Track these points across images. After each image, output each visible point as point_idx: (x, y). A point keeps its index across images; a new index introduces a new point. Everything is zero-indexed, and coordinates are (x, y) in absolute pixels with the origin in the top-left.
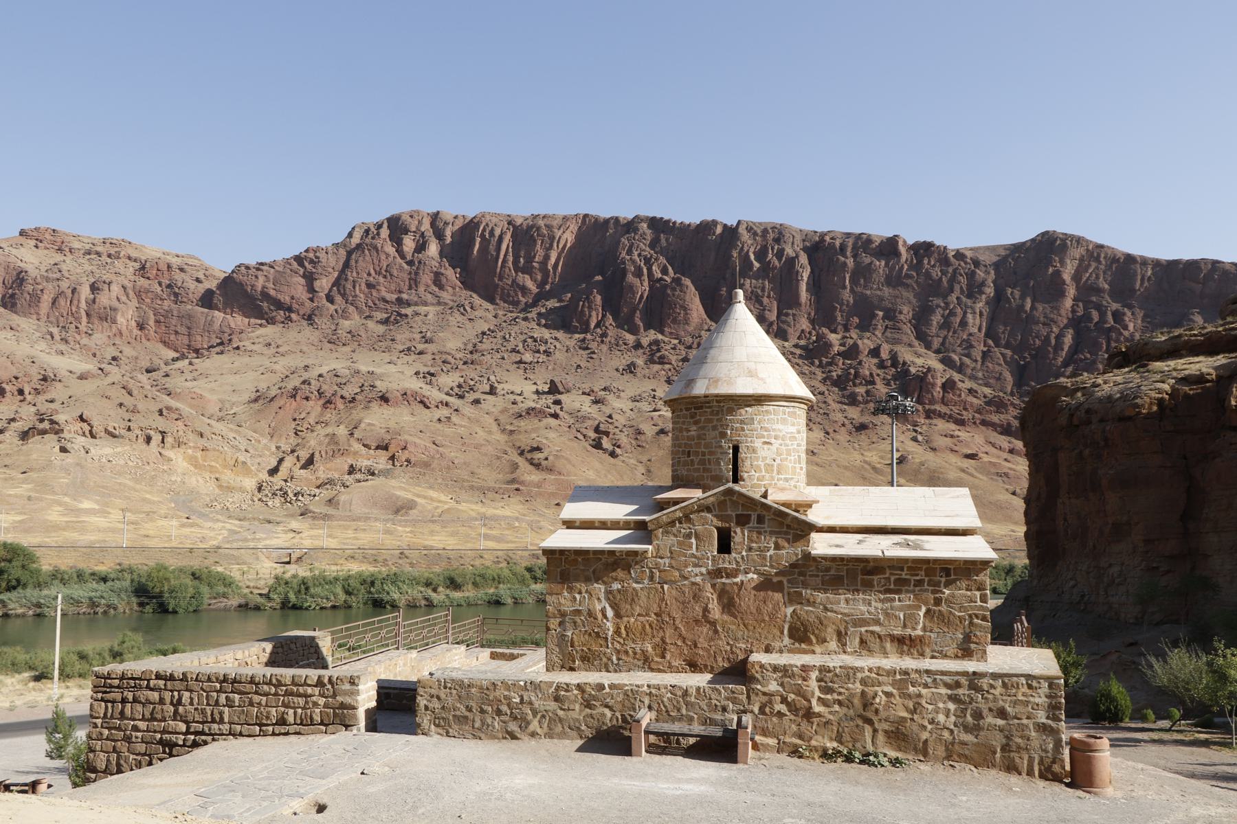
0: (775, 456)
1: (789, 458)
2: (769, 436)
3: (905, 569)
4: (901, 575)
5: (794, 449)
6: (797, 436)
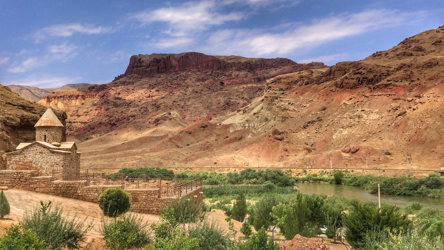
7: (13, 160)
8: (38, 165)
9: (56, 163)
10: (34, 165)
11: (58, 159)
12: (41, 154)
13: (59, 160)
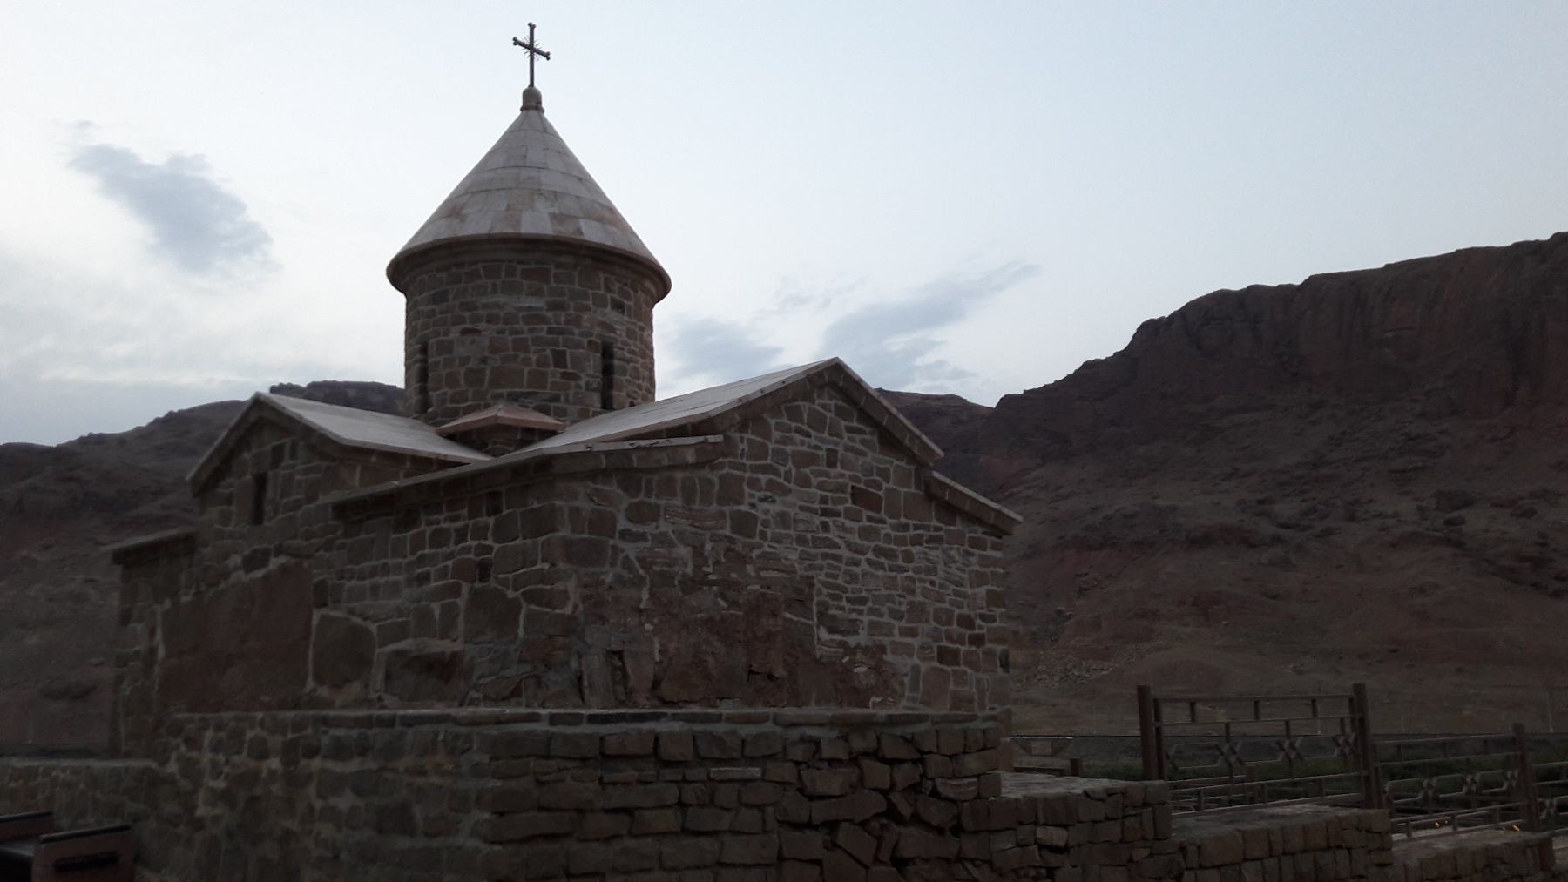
0: (486, 354)
1: (522, 355)
2: (476, 319)
5: (537, 341)
6: (550, 315)
7: (631, 550)
8: (852, 641)
9: (966, 622)
10: (824, 634)
11: (980, 579)
12: (866, 513)
13: (982, 591)
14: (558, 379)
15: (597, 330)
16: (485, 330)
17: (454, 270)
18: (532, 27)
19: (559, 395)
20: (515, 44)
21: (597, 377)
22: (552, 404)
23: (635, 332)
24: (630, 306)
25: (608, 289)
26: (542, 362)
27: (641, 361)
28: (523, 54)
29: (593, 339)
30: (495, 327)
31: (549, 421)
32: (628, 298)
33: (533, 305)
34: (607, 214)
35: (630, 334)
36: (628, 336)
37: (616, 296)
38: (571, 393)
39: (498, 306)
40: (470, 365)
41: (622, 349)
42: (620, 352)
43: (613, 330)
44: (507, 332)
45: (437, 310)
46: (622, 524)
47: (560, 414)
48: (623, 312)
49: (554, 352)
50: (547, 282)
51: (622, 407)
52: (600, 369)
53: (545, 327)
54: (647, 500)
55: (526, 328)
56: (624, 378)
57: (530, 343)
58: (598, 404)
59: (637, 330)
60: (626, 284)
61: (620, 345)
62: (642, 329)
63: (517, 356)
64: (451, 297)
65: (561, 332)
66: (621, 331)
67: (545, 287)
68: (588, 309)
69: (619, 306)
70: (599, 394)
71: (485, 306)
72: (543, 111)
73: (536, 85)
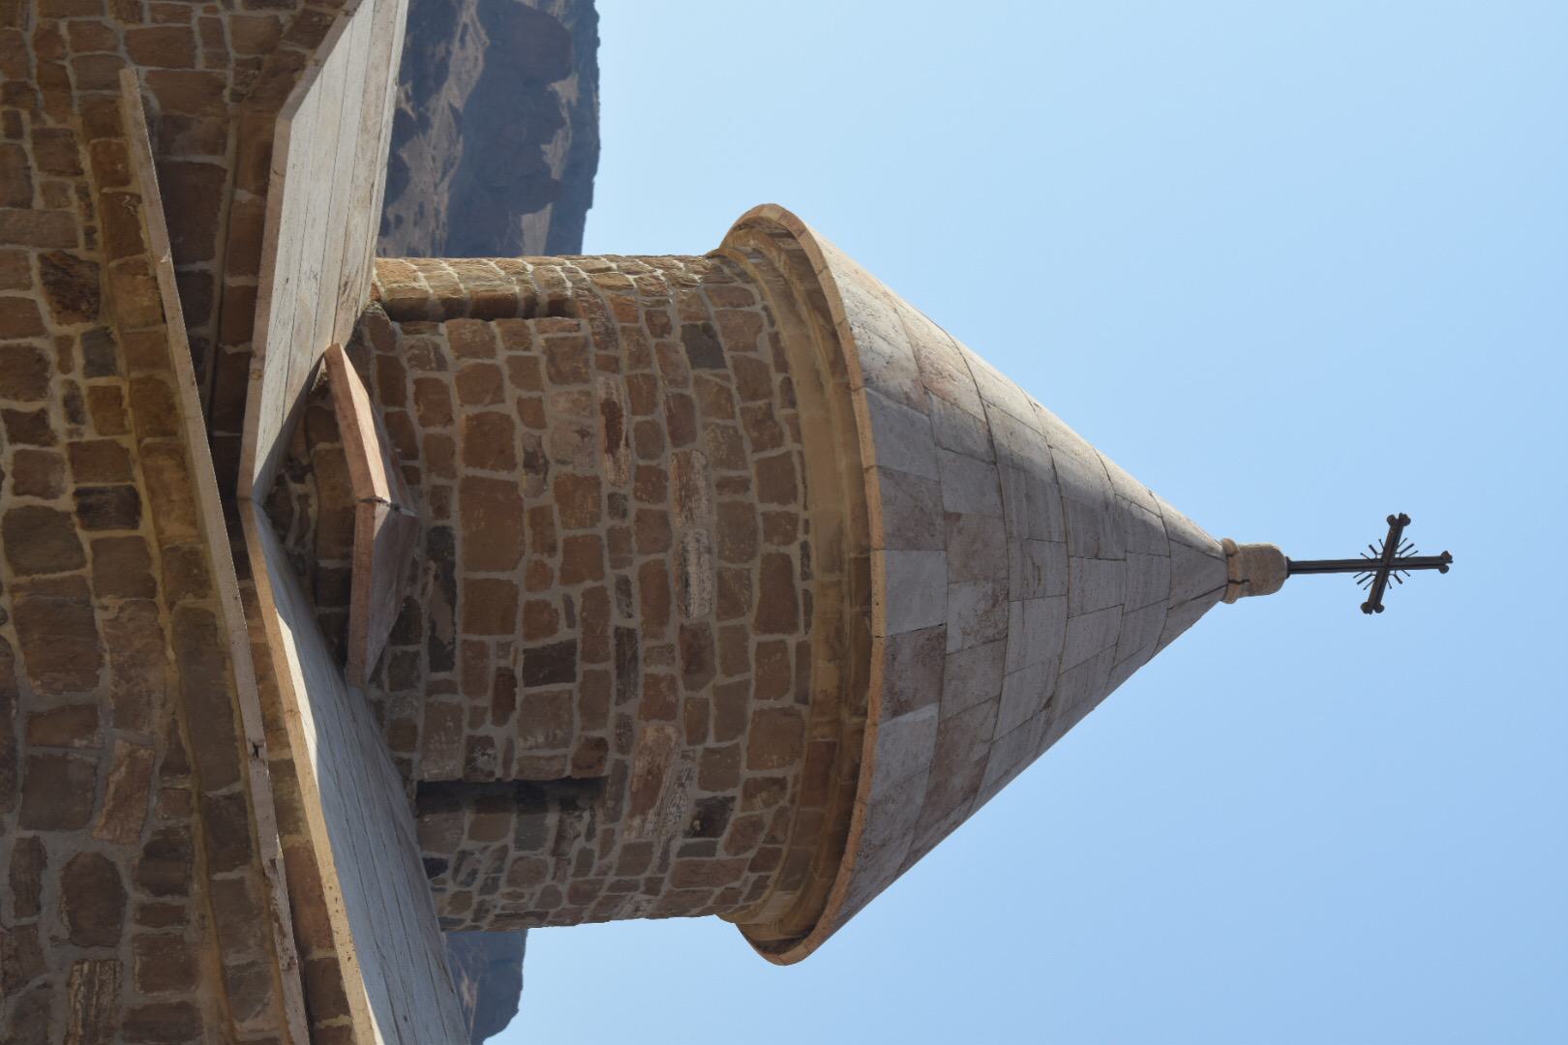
0: (555, 470)
1: (555, 563)
2: (649, 440)
3: (101, 381)
4: (65, 366)
5: (597, 601)
6: (671, 634)
14: (494, 663)
15: (638, 765)
16: (616, 462)
17: (777, 379)
18: (1442, 563)
19: (450, 667)
20: (1391, 520)
21: (507, 764)
22: (422, 648)
23: (644, 866)
24: (710, 850)
25: (751, 790)
26: (540, 618)
27: (564, 888)
28: (1369, 540)
29: (613, 755)
30: (627, 490)
31: (371, 638)
32: (734, 847)
33: (694, 589)
34: (959, 781)
35: (638, 854)
36: (628, 848)
37: (736, 814)
38: (459, 698)
39: (687, 492)
40: (520, 429)
41: (590, 834)
42: (582, 827)
43: (640, 809)
44: (617, 522)
45: (669, 339)
46: (59, 846)
47: (398, 672)
48: (692, 832)
49: (569, 647)
50: (765, 624)
51: (423, 839)
52: (530, 775)
53: (635, 623)
54: (130, 911)
55: (631, 573)
56: (509, 840)
57: (589, 584)
58: (430, 771)
59: (648, 874)
60: (772, 839)
61: (600, 828)
62: (652, 887)
63: (552, 549)
64: (706, 374)
65: (626, 664)
66: (630, 830)
67: (749, 619)
68: (696, 734)
69: (709, 819)
70: (460, 775)
71: (684, 465)
72: (1229, 599)
73: (1295, 579)
